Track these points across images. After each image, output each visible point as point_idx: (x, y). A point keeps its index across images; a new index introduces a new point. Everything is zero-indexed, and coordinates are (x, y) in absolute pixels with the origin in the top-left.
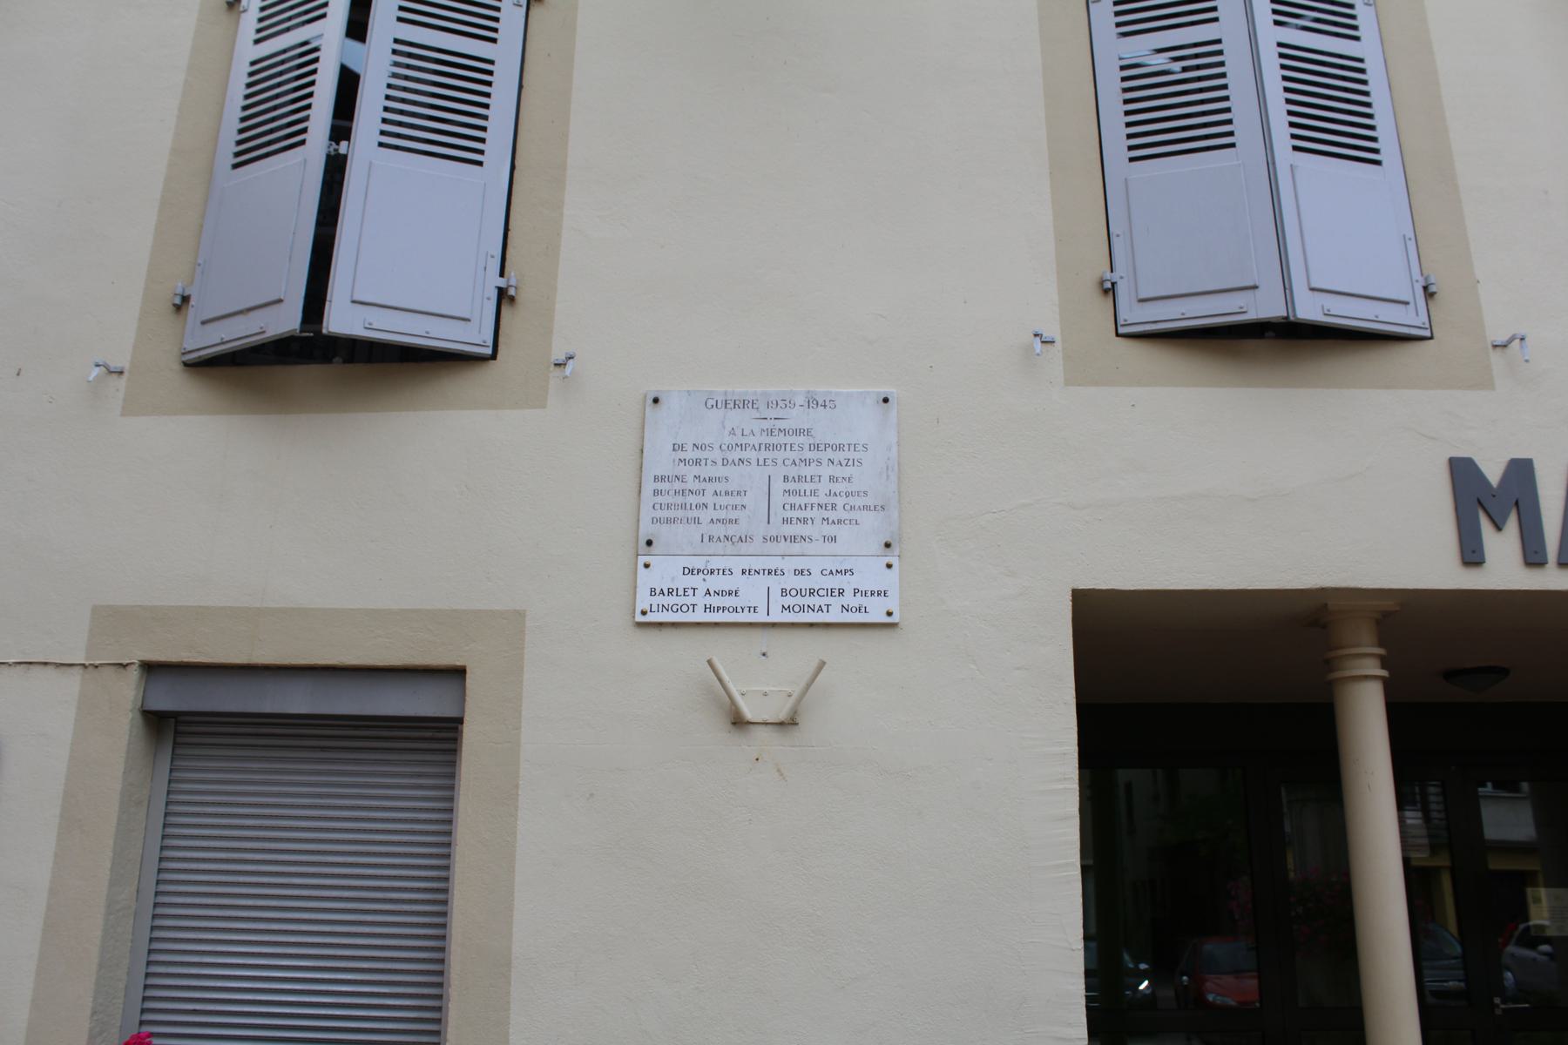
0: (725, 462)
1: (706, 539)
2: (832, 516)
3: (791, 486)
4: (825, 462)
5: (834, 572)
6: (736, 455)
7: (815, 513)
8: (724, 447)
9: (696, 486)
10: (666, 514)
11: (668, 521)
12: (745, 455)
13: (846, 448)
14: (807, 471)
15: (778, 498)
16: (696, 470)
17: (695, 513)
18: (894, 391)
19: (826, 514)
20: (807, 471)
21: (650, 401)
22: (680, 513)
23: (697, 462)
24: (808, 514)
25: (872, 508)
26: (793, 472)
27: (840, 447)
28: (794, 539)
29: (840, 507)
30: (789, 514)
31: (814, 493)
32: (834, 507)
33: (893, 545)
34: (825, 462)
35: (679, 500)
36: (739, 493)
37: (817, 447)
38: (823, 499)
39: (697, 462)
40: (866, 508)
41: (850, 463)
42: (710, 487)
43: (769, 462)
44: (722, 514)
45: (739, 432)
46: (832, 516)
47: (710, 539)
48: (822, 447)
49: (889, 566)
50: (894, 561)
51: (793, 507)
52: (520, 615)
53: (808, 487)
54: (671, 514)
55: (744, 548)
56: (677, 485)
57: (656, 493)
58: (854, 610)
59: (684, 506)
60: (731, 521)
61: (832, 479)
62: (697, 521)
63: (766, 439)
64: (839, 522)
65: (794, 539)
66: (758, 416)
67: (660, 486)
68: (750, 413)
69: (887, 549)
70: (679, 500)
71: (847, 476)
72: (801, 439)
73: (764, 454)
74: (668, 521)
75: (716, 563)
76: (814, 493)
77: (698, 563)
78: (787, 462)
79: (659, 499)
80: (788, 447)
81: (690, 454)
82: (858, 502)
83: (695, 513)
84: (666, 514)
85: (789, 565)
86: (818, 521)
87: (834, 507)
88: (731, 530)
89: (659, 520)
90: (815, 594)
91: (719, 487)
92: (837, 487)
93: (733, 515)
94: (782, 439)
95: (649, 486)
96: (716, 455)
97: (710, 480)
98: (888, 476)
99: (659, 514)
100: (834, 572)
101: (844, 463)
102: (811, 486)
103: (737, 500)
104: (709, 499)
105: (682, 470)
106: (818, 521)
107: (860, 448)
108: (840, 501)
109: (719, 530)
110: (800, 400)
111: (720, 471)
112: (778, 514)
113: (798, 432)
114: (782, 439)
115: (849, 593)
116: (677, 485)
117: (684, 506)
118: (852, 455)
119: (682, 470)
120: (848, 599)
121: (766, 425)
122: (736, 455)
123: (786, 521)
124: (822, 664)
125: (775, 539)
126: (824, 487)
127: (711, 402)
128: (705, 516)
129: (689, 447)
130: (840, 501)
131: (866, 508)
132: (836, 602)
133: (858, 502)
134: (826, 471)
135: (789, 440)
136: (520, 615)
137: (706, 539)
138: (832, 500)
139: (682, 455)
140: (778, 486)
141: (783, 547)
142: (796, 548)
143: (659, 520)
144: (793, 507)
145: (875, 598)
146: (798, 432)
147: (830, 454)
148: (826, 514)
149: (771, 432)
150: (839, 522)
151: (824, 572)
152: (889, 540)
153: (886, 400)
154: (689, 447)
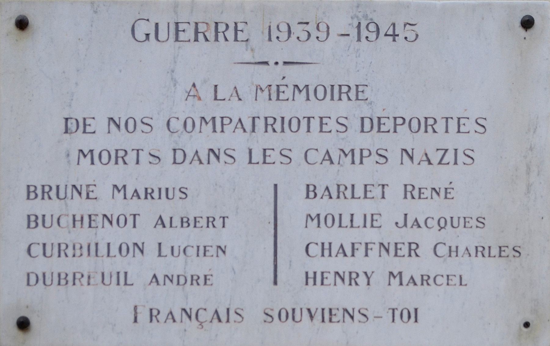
1: (144, 316)
4: (394, 156)
13: (440, 126)
19: (396, 264)
25: (495, 251)
29: (425, 250)
34: (394, 156)
36: (210, 222)
41: (449, 157)
43: (274, 156)
48: (389, 125)
60: (195, 280)
64: (425, 280)
71: (441, 185)
80: (315, 124)
98: (529, 186)
101: (435, 158)
102: (369, 207)
107: (469, 126)
137: (144, 316)
148: (396, 264)
150: (425, 280)
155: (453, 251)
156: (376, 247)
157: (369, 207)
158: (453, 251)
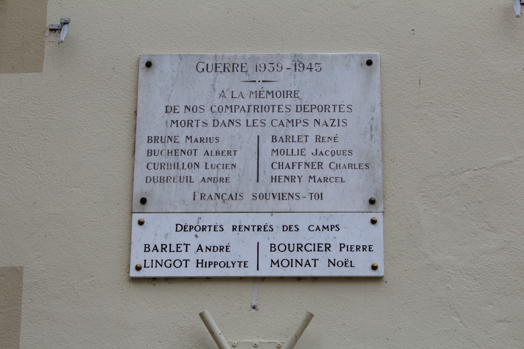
0: (216, 123)
1: (198, 197)
2: (319, 174)
3: (279, 145)
4: (311, 123)
5: (321, 228)
6: (226, 116)
7: (304, 172)
8: (215, 109)
9: (188, 146)
10: (159, 173)
11: (162, 180)
12: (234, 116)
13: (332, 109)
14: (294, 131)
15: (266, 157)
16: (188, 131)
17: (187, 172)
18: (378, 53)
19: (312, 172)
20: (294, 131)
21: (143, 65)
22: (173, 173)
23: (189, 123)
24: (295, 172)
25: (357, 166)
26: (281, 132)
27: (325, 108)
28: (282, 196)
29: (326, 165)
30: (278, 172)
31: (301, 152)
32: (320, 165)
33: (377, 201)
34: (311, 123)
35: (172, 159)
36: (229, 153)
37: (304, 108)
38: (310, 158)
39: (189, 123)
40: (351, 166)
41: (336, 123)
42: (201, 148)
43: (258, 123)
44: (213, 173)
45: (228, 95)
46: (319, 174)
47: (202, 197)
48: (309, 108)
49: (374, 222)
50: (379, 217)
51: (281, 165)
52: (18, 271)
53: (295, 146)
54: (164, 173)
55: (234, 205)
56: (170, 146)
57: (150, 153)
58: (340, 264)
59: (176, 166)
60: (221, 180)
61: (318, 139)
62: (189, 180)
63: (254, 101)
64: (326, 179)
65: (282, 196)
66: (247, 78)
67: (153, 146)
68: (239, 76)
69: (372, 206)
70: (172, 159)
71: (332, 135)
72: (288, 101)
73: (253, 115)
74: (162, 180)
75: (208, 220)
76: (301, 152)
77: (191, 220)
78: (275, 123)
79: (153, 159)
80: (276, 108)
81: (183, 116)
82: (344, 160)
83: (187, 172)
84: (159, 173)
85: (277, 221)
86: (305, 179)
87: (320, 165)
88: (222, 188)
89: (153, 179)
90: (303, 249)
91: (211, 147)
92: (323, 147)
93: (223, 174)
94: (269, 101)
95: (143, 147)
96: (208, 116)
97: (202, 140)
98: (372, 136)
99: (152, 173)
100: (321, 228)
102: (300, 146)
103: (227, 160)
104: (200, 158)
105: (174, 130)
106: (305, 179)
107: (345, 109)
108: (326, 160)
109: (210, 189)
110: (287, 63)
111: (211, 132)
112: (267, 173)
113: (285, 94)
114: (269, 101)
115: (335, 248)
116: (170, 146)
117: (176, 166)
118: (337, 115)
119: (174, 130)
120: (335, 254)
121: (254, 87)
122: (226, 116)
123: (275, 179)
124: (310, 317)
125: (264, 196)
126: (310, 146)
127: (201, 66)
128: (197, 174)
129: (181, 109)
130: (326, 160)
131: (351, 166)
132: (323, 257)
133: (344, 160)
134: (313, 131)
135: (276, 101)
136: (18, 271)
137: (198, 197)
138: (319, 159)
139: (174, 117)
140: (267, 146)
141: (271, 204)
142: (284, 205)
143: (153, 179)
144: (281, 165)
145: (361, 253)
146: (285, 94)
147: (316, 115)
148: (312, 172)
149: (259, 94)
150: (326, 179)
151: (311, 228)
152: (373, 196)
153: (369, 63)
154: (181, 109)
155: (338, 166)
156: (303, 164)
157: (300, 146)
158: (338, 166)
